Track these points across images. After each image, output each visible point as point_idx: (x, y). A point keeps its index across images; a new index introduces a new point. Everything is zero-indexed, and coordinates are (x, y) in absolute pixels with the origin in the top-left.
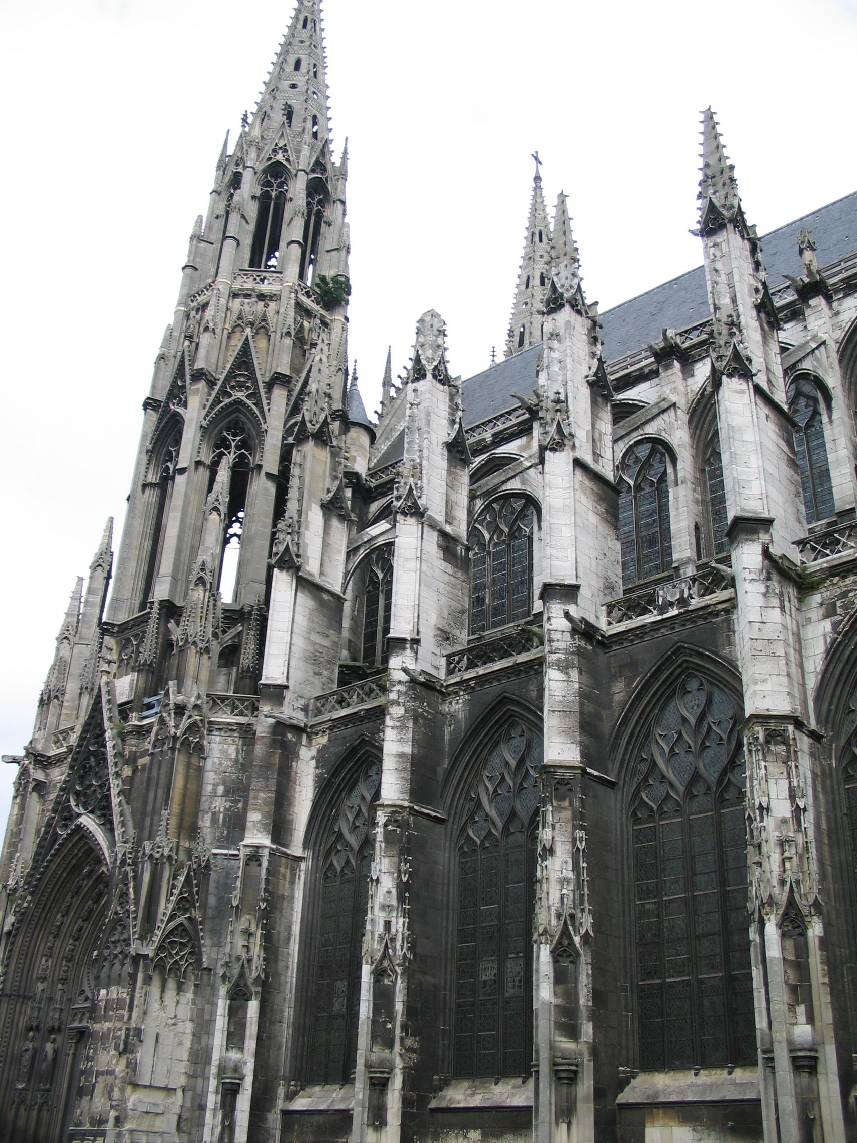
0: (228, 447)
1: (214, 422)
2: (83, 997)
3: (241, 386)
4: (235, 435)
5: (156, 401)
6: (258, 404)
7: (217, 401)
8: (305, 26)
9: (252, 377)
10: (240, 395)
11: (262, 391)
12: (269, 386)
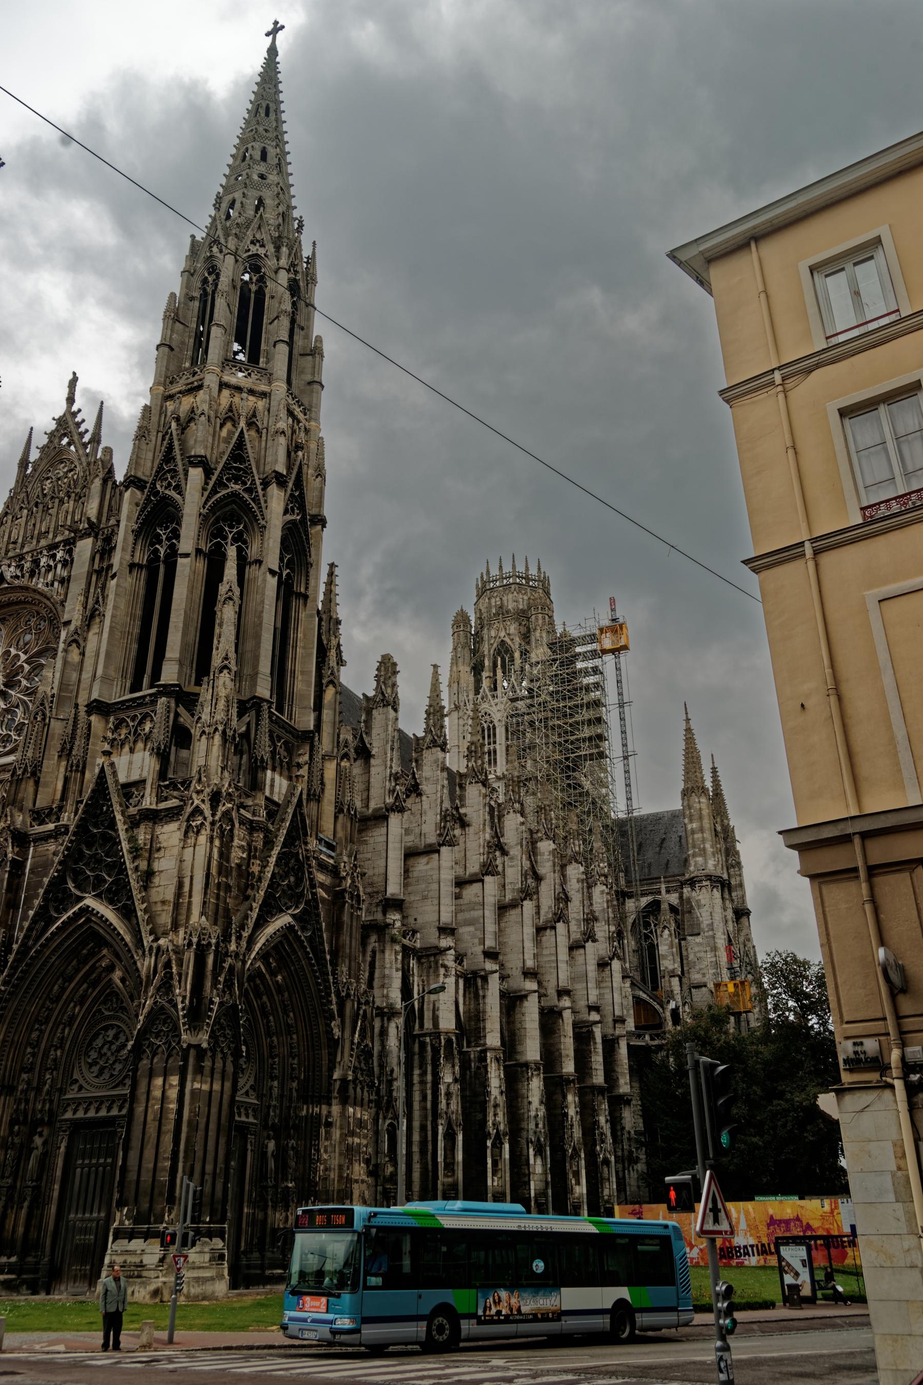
0: (225, 538)
1: (212, 510)
2: (75, 1087)
3: (236, 479)
4: (231, 527)
5: (140, 480)
6: (256, 500)
7: (214, 491)
8: (267, 114)
9: (248, 471)
10: (235, 487)
11: (259, 488)
12: (266, 484)
